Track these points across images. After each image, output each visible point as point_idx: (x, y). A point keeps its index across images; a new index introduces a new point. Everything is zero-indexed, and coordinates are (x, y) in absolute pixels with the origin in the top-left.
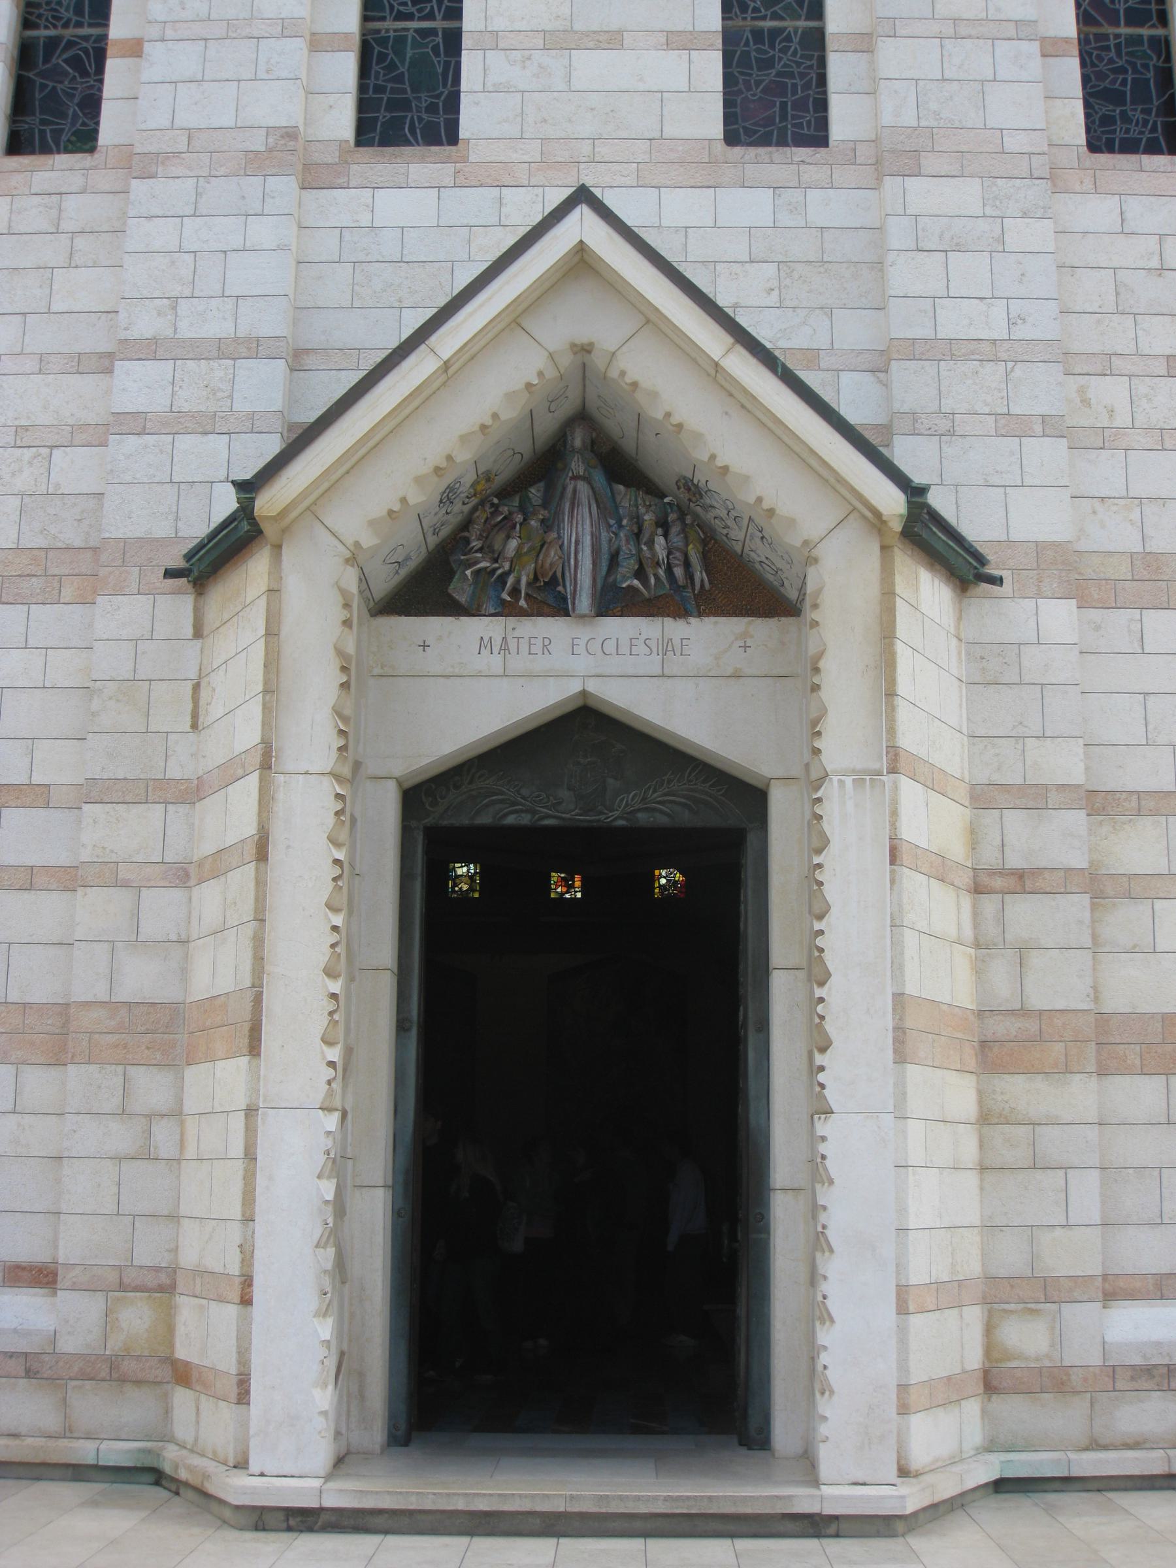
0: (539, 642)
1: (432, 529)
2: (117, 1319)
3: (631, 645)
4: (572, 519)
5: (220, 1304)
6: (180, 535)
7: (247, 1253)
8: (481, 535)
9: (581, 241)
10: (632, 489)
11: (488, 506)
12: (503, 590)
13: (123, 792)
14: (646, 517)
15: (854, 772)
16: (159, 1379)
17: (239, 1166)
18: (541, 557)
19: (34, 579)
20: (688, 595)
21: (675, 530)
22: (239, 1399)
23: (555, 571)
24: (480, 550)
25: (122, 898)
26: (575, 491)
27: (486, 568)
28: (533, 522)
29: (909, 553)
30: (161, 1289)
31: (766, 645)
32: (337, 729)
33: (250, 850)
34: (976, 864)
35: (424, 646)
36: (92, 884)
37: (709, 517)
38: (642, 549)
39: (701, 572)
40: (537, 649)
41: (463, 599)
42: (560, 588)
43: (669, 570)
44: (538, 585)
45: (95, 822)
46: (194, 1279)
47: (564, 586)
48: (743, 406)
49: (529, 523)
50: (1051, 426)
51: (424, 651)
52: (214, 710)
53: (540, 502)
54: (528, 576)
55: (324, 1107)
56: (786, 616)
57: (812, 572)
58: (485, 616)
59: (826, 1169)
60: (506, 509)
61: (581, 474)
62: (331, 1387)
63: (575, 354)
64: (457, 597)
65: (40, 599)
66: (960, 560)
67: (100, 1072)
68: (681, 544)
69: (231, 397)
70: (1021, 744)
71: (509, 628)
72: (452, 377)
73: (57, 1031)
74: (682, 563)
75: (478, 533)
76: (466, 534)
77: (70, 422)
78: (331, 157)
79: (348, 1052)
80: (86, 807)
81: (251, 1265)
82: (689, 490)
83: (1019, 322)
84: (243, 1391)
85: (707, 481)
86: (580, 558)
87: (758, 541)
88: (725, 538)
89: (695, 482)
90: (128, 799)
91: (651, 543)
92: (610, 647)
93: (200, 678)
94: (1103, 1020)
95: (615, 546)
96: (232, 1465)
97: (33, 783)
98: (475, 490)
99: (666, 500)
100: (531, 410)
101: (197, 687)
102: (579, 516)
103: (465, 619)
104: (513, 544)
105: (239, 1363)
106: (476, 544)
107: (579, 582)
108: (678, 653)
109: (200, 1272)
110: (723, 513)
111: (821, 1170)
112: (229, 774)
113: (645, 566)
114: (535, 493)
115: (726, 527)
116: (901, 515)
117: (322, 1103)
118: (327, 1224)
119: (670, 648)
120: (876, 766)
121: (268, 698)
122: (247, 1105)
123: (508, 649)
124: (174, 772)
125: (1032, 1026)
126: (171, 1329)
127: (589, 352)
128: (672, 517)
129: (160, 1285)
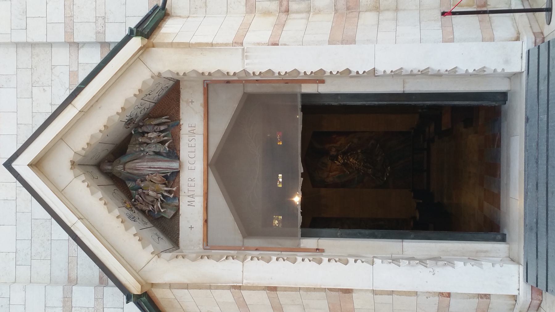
1: (145, 225)
3: (191, 147)
4: (141, 170)
7: (430, 294)
8: (147, 206)
9: (28, 165)
11: (135, 203)
17: (395, 296)
21: (146, 130)
23: (162, 176)
24: (153, 206)
27: (160, 204)
28: (142, 185)
31: (191, 94)
37: (140, 116)
39: (162, 119)
40: (192, 183)
41: (173, 213)
42: (169, 174)
47: (168, 173)
53: (134, 183)
55: (372, 264)
58: (179, 204)
60: (137, 196)
62: (483, 263)
64: (172, 215)
66: (157, 16)
68: (151, 127)
74: (159, 126)
75: (146, 207)
76: (147, 211)
79: (351, 256)
82: (129, 123)
86: (157, 167)
87: (150, 96)
92: (192, 155)
95: (152, 153)
96: (515, 302)
98: (129, 208)
99: (133, 133)
104: (151, 193)
106: (151, 208)
107: (166, 167)
108: (194, 128)
110: (139, 110)
114: (130, 185)
115: (144, 109)
117: (371, 265)
120: (240, 51)
121: (213, 288)
123: (193, 195)
128: (140, 130)
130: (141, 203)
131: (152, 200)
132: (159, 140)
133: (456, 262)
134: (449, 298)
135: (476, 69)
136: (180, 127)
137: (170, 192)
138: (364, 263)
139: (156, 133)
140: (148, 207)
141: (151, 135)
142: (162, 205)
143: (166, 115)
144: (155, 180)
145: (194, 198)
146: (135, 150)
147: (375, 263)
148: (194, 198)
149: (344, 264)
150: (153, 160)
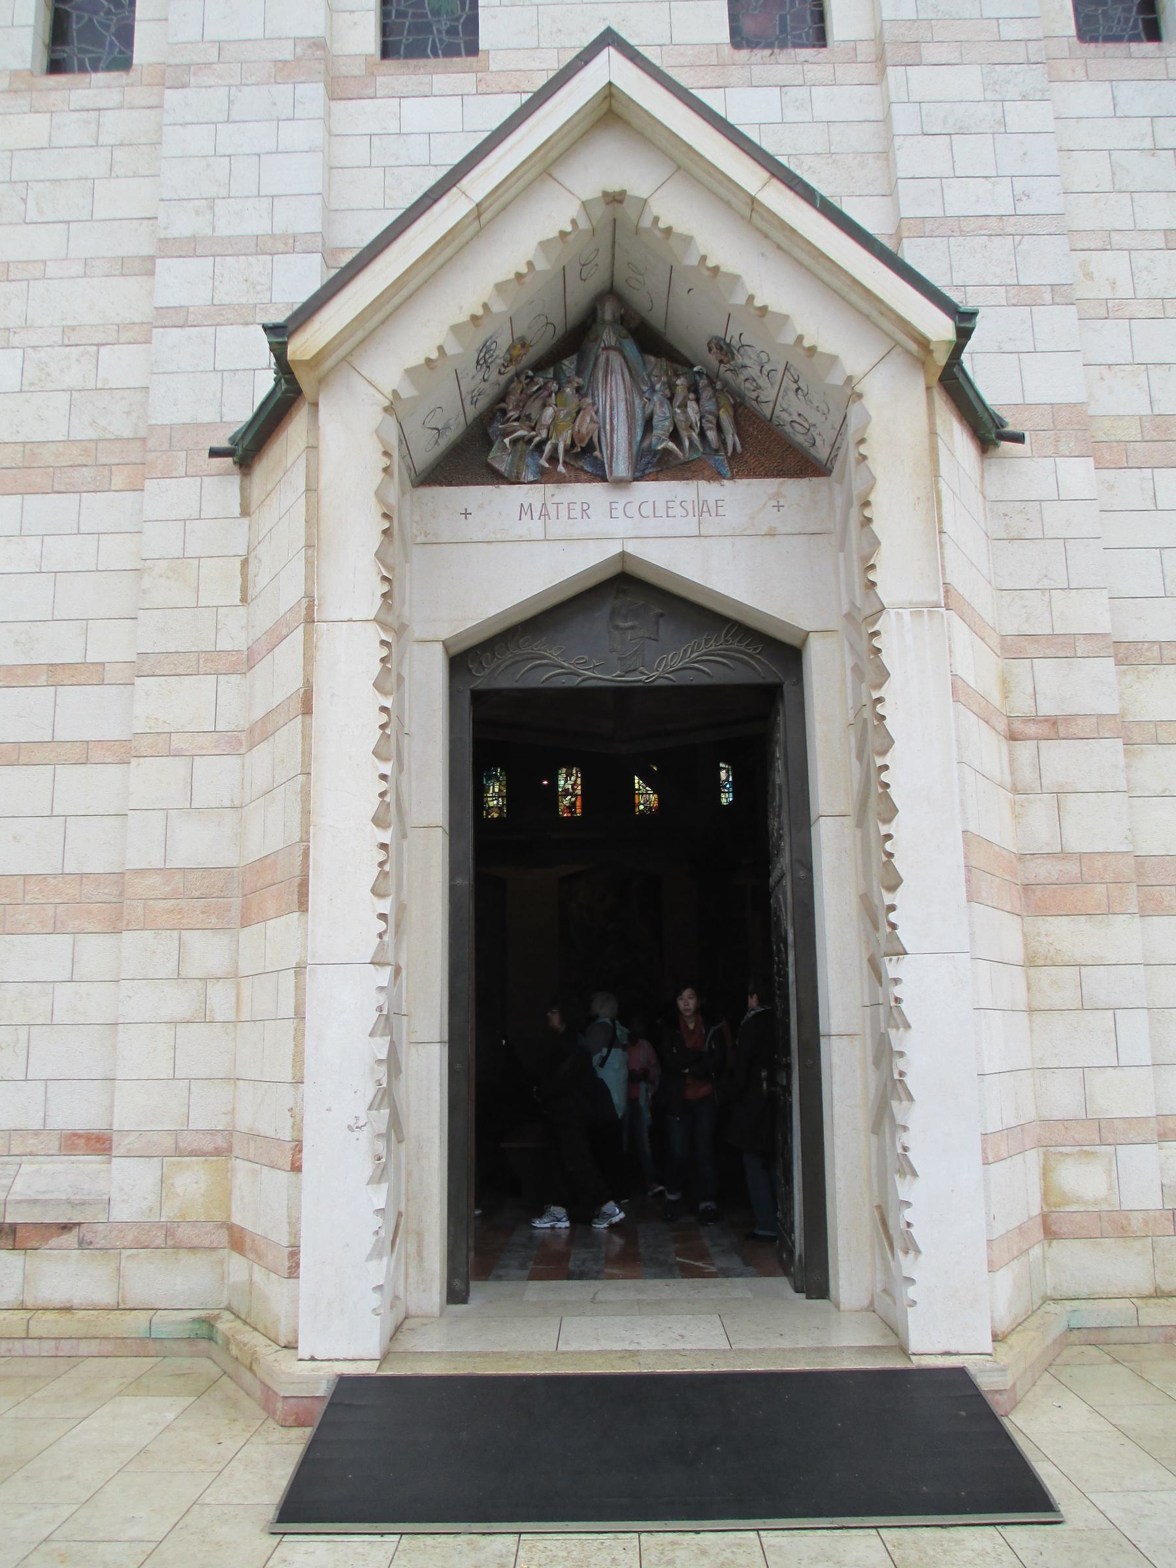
0: (578, 508)
1: (470, 396)
2: (173, 1185)
3: (668, 508)
4: (606, 387)
5: (272, 1169)
6: (224, 420)
7: (296, 1117)
8: (517, 405)
10: (663, 359)
12: (541, 457)
13: (175, 665)
14: (678, 382)
15: (912, 605)
16: (214, 1245)
17: (290, 1025)
18: (577, 423)
19: (84, 469)
20: (721, 458)
21: (706, 394)
22: (290, 1273)
23: (591, 438)
24: (517, 420)
25: (177, 767)
26: (607, 359)
29: (944, 398)
30: (217, 1152)
31: (798, 504)
32: (380, 576)
33: (297, 705)
34: (1010, 712)
35: (466, 514)
36: (145, 755)
38: (675, 412)
39: (733, 435)
40: (576, 512)
41: (502, 467)
42: (597, 453)
43: (702, 434)
44: (575, 451)
45: (147, 695)
46: (248, 1143)
47: (601, 451)
48: (779, 247)
49: (565, 391)
50: (1060, 294)
51: (466, 518)
52: (261, 577)
54: (565, 441)
55: (376, 961)
56: (817, 476)
57: (854, 411)
58: (524, 483)
59: (901, 1013)
61: (613, 344)
62: (385, 1259)
63: (608, 203)
64: (496, 466)
65: (92, 487)
67: (155, 938)
69: (271, 289)
70: (1048, 596)
71: (548, 494)
72: (485, 225)
73: (114, 900)
74: (714, 427)
75: (515, 404)
76: (502, 405)
77: (117, 321)
78: (358, 69)
79: (401, 908)
80: (138, 681)
81: (301, 1130)
82: (721, 349)
83: (1024, 198)
84: (294, 1265)
85: (741, 334)
86: (615, 422)
87: (792, 394)
88: (754, 403)
89: (728, 341)
90: (179, 671)
91: (683, 406)
92: (647, 510)
93: (248, 554)
94: (1140, 860)
95: (648, 411)
96: (283, 1345)
97: (88, 661)
98: (511, 355)
99: (695, 369)
100: (564, 267)
101: (245, 563)
102: (613, 383)
103: (505, 488)
104: (549, 411)
105: (290, 1234)
106: (513, 414)
108: (713, 513)
109: (254, 1136)
110: (754, 371)
111: (896, 1015)
112: (275, 637)
113: (680, 429)
115: (759, 387)
116: (950, 342)
117: (373, 957)
118: (381, 1085)
119: (705, 509)
122: (297, 964)
123: (548, 515)
124: (225, 644)
125: (1073, 868)
126: (228, 1193)
127: (620, 202)
128: (703, 382)
129: (216, 1149)
130: (524, 392)
131: (533, 416)
132: (682, 427)
133: (385, 1186)
134: (289, 1169)
135: (911, 1230)
136: (714, 480)
137: (553, 459)
138: (379, 940)
139: (698, 419)
140: (514, 409)
141: (693, 409)
142: (521, 442)
143: (742, 447)
144: (583, 420)
145: (539, 519)
146: (654, 373)
147: (377, 970)
148: (539, 519)
149: (374, 886)
150: (631, 417)
